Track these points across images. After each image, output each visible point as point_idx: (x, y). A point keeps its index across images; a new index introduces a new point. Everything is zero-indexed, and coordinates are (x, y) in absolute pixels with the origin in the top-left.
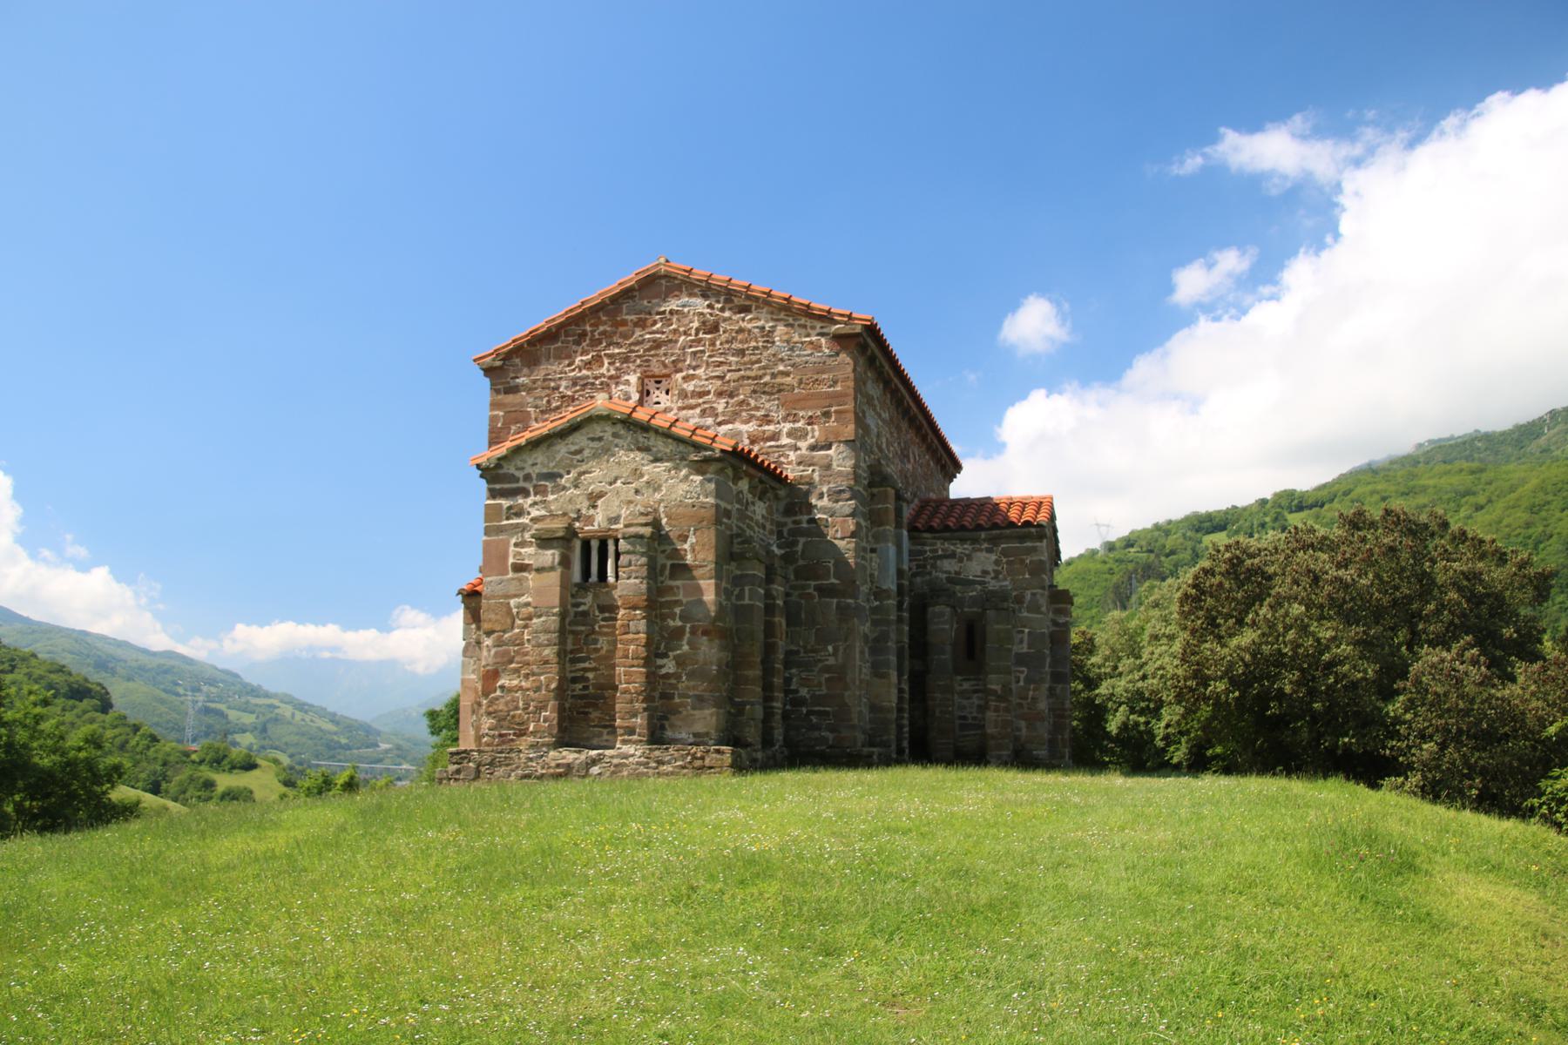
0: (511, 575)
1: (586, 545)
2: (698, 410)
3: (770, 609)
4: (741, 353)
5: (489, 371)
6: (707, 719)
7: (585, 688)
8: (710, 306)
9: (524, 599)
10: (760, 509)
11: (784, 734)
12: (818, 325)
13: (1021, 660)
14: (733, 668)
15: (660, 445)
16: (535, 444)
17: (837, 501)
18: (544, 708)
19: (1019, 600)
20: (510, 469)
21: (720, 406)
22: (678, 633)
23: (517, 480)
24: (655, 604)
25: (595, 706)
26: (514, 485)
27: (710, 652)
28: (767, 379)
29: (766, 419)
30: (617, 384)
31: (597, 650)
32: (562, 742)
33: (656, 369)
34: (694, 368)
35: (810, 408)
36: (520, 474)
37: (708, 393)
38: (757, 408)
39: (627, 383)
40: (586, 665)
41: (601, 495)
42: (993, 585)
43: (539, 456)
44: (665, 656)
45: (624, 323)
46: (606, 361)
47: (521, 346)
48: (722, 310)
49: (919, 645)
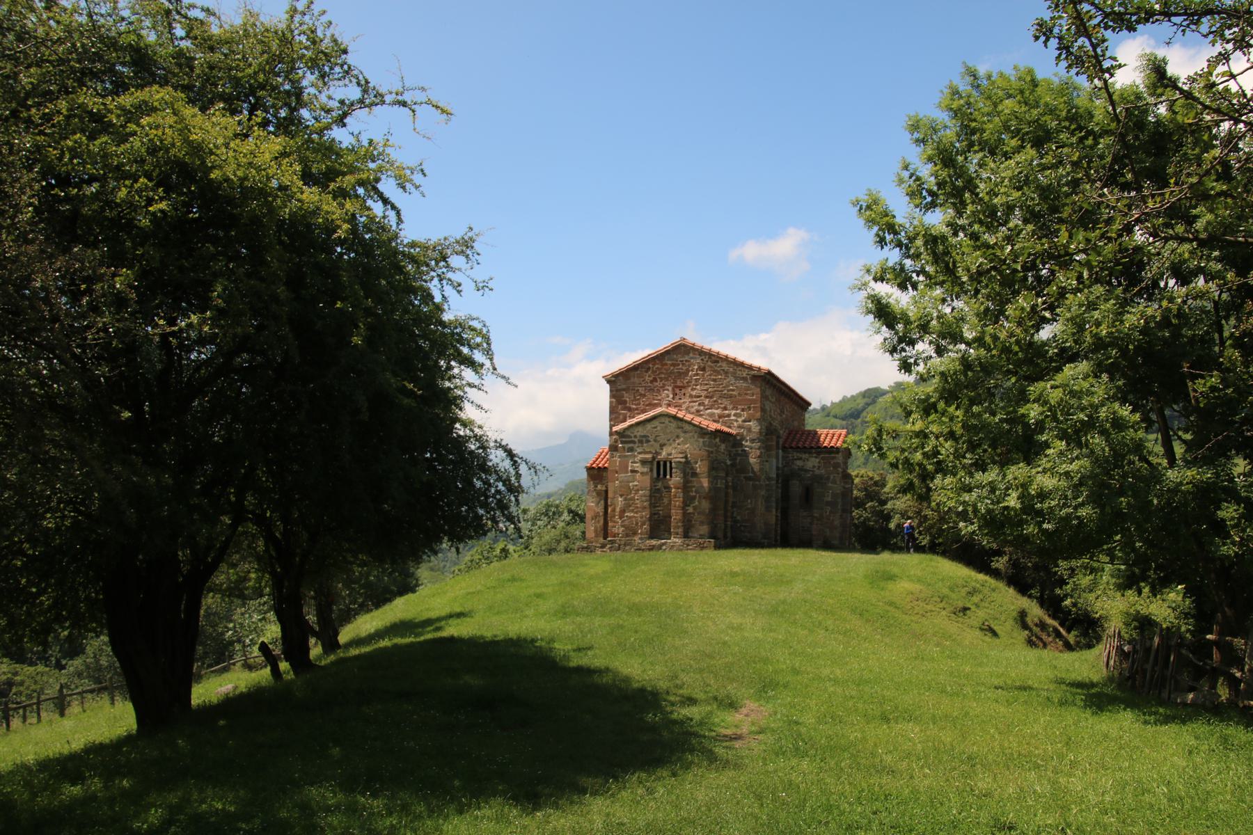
1: (658, 463)
3: (727, 487)
4: (714, 380)
5: (609, 382)
6: (704, 529)
10: (723, 447)
11: (732, 534)
13: (828, 503)
14: (713, 510)
15: (687, 427)
16: (638, 424)
19: (828, 478)
20: (628, 433)
22: (694, 498)
24: (686, 487)
27: (706, 505)
29: (725, 409)
32: (651, 537)
33: (679, 383)
42: (817, 472)
49: (785, 496)
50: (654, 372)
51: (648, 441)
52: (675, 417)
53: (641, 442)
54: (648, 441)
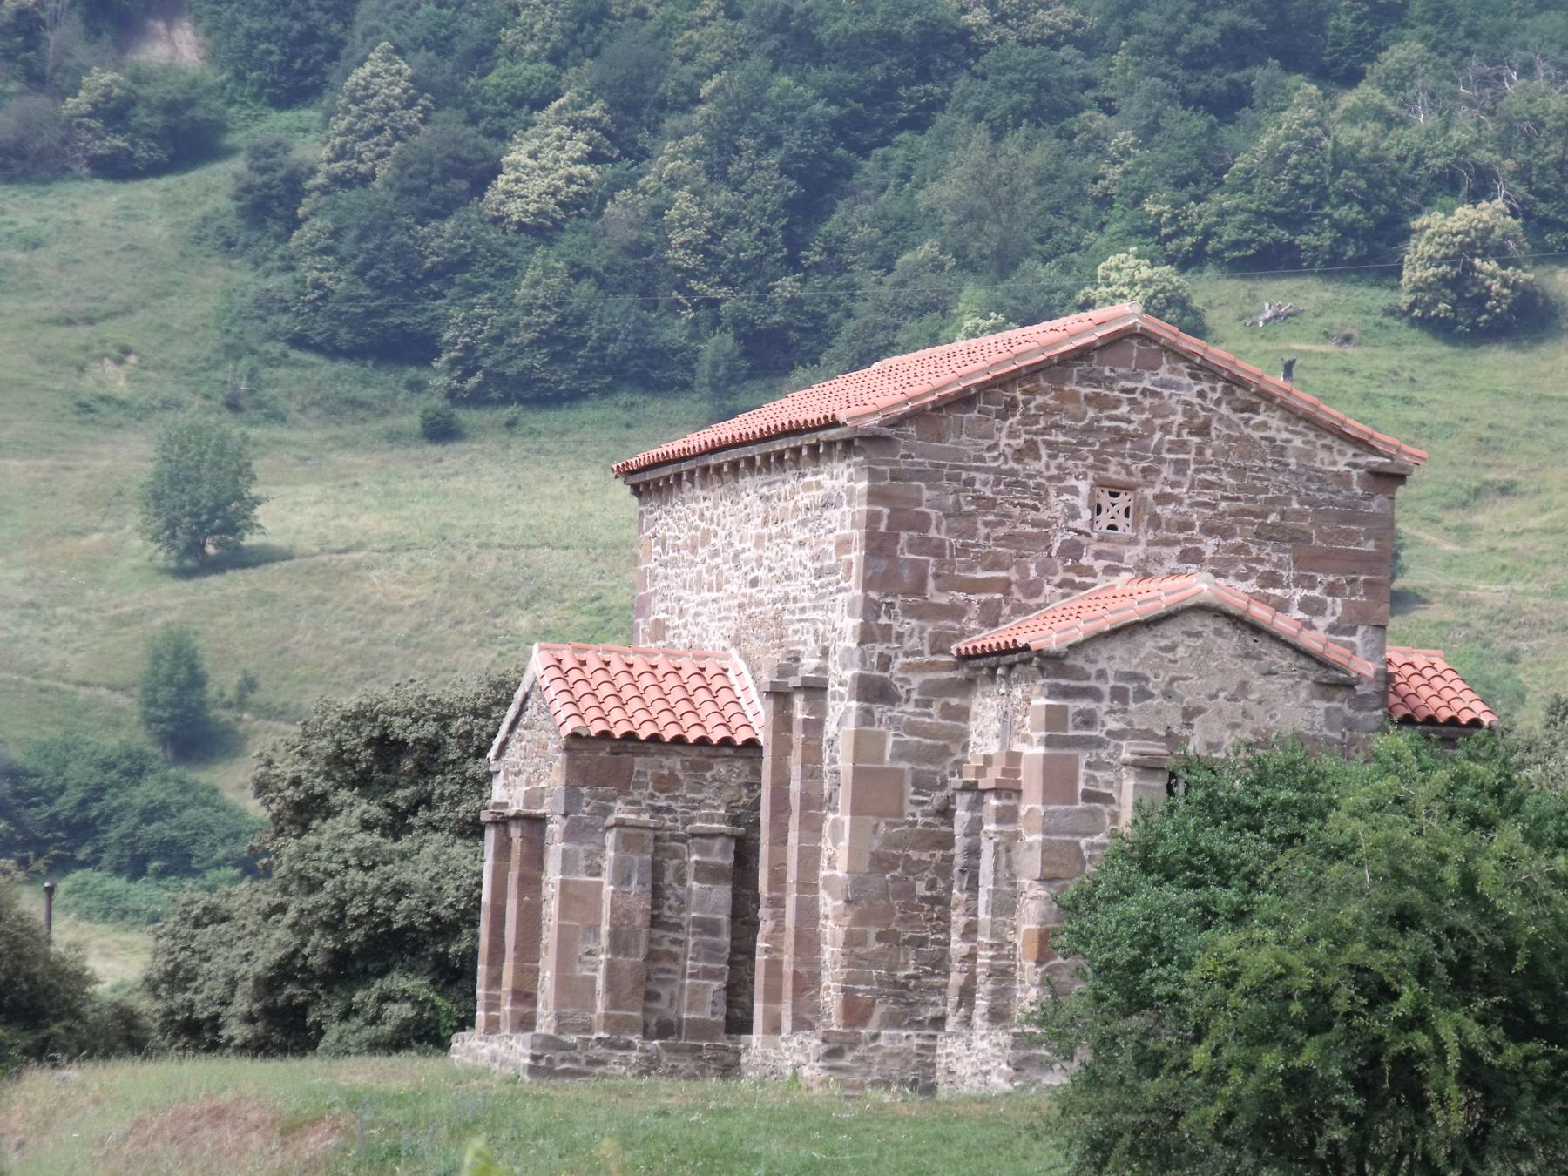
0: (1081, 805)
2: (1177, 550)
4: (1238, 472)
8: (1201, 394)
9: (1096, 839)
12: (1351, 451)
15: (1276, 657)
17: (1359, 709)
20: (1078, 661)
21: (1209, 546)
23: (1088, 678)
26: (1084, 684)
28: (1273, 518)
29: (1272, 580)
30: (1060, 492)
33: (1114, 472)
34: (1173, 485)
35: (1335, 572)
36: (1092, 669)
37: (1191, 526)
38: (1260, 561)
39: (1074, 491)
41: (1199, 711)
43: (1118, 648)
45: (1074, 396)
46: (1044, 452)
47: (923, 408)
48: (1218, 402)
50: (1029, 420)
51: (1144, 695)
52: (1239, 621)
53: (1119, 694)
54: (1144, 695)
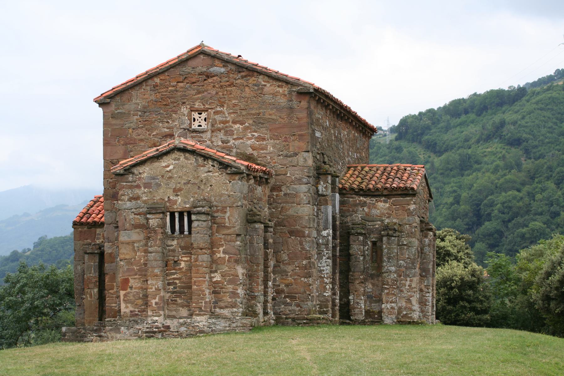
7: (175, 288)
18: (155, 299)
25: (180, 297)
31: (180, 269)
33: (197, 105)
37: (228, 122)
40: (175, 276)
41: (180, 190)
44: (216, 271)
